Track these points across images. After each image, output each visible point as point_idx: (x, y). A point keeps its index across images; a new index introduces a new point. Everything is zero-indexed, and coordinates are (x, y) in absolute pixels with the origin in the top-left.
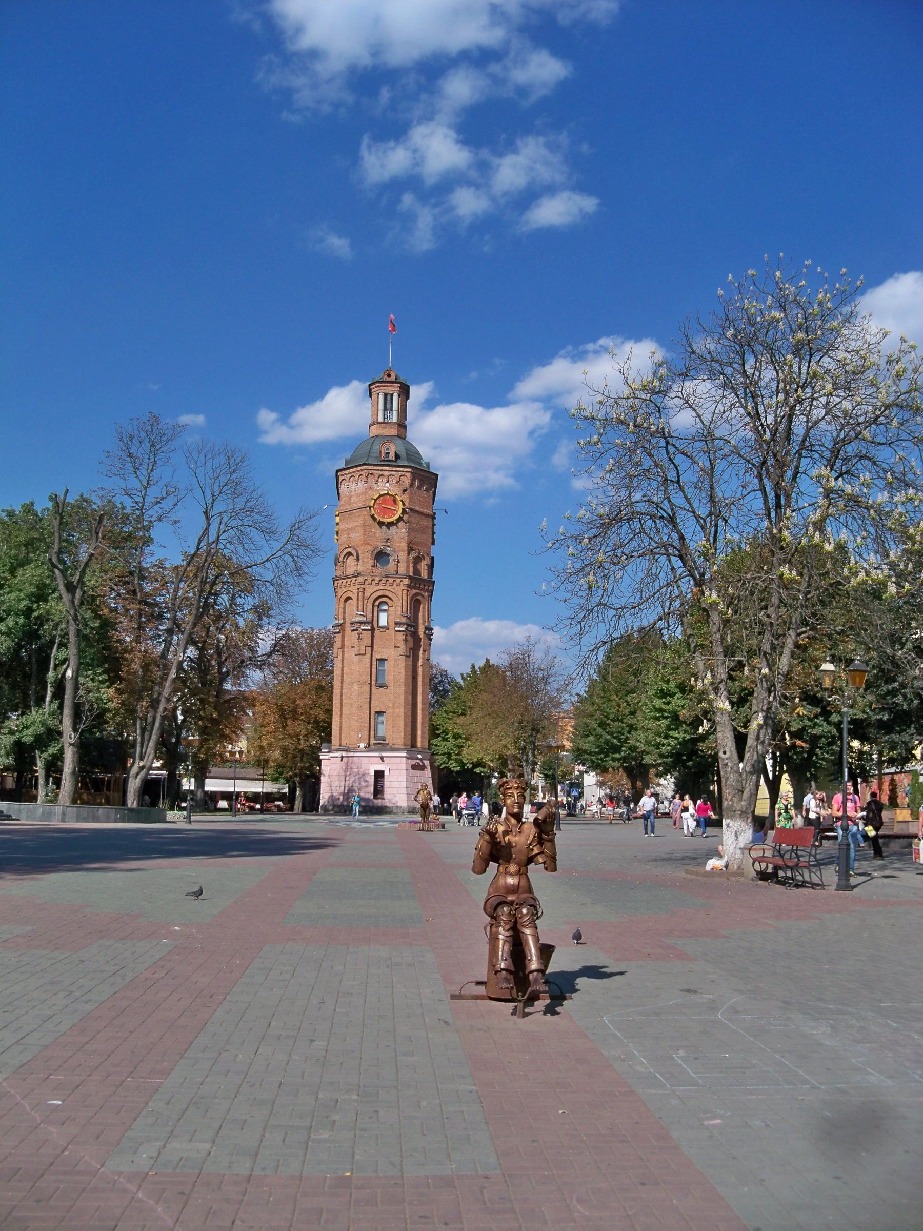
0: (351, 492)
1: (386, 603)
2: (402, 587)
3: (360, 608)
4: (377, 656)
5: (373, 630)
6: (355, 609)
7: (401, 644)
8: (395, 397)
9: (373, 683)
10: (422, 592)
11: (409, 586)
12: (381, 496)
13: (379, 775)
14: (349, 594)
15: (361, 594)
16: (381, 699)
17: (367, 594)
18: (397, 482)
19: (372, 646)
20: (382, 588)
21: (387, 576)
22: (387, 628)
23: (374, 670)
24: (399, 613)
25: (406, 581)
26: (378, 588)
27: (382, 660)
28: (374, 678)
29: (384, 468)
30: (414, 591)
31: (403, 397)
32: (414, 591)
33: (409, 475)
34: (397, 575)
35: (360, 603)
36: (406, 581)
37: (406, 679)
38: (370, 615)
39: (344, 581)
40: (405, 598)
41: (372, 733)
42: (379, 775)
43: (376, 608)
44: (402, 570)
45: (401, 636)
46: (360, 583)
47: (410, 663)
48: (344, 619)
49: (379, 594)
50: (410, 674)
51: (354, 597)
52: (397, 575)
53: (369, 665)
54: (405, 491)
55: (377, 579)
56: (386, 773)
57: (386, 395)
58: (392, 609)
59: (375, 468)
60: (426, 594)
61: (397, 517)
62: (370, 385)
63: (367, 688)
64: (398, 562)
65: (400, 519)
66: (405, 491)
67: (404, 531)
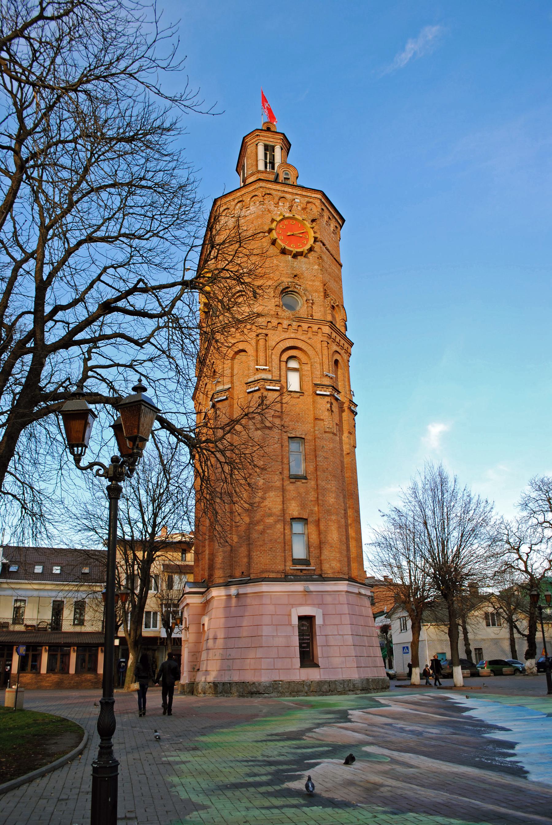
3: (262, 360)
6: (252, 364)
8: (278, 150)
12: (284, 218)
14: (241, 346)
15: (262, 342)
17: (272, 343)
20: (293, 335)
24: (318, 373)
26: (286, 335)
33: (318, 203)
35: (261, 354)
48: (232, 383)
51: (251, 350)
54: (313, 221)
55: (285, 323)
56: (319, 621)
58: (307, 368)
60: (345, 356)
61: (308, 247)
62: (244, 138)
64: (313, 304)
66: (313, 221)
67: (316, 267)
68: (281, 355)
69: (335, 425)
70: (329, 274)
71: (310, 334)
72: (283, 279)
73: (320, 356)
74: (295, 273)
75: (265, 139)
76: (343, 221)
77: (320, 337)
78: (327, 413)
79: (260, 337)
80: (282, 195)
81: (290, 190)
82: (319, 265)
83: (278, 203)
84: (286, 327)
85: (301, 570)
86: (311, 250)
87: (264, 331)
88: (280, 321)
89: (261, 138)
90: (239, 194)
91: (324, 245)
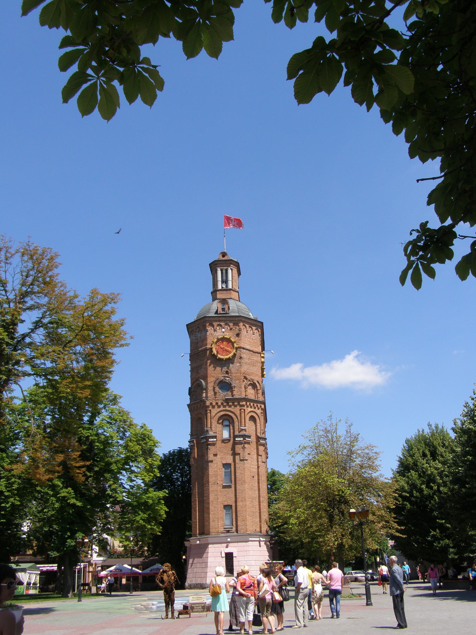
0: (197, 339)
13: (229, 557)
16: (227, 497)
17: (213, 414)
20: (224, 409)
22: (229, 440)
30: (250, 409)
31: (235, 271)
32: (250, 409)
39: (196, 406)
42: (229, 557)
49: (222, 413)
57: (222, 270)
67: (238, 364)
68: (219, 420)
69: (246, 454)
70: (249, 364)
72: (220, 375)
73: (239, 418)
75: (221, 265)
76: (262, 323)
80: (219, 323)
82: (240, 363)
86: (235, 355)
89: (219, 265)
90: (197, 323)
91: (244, 348)
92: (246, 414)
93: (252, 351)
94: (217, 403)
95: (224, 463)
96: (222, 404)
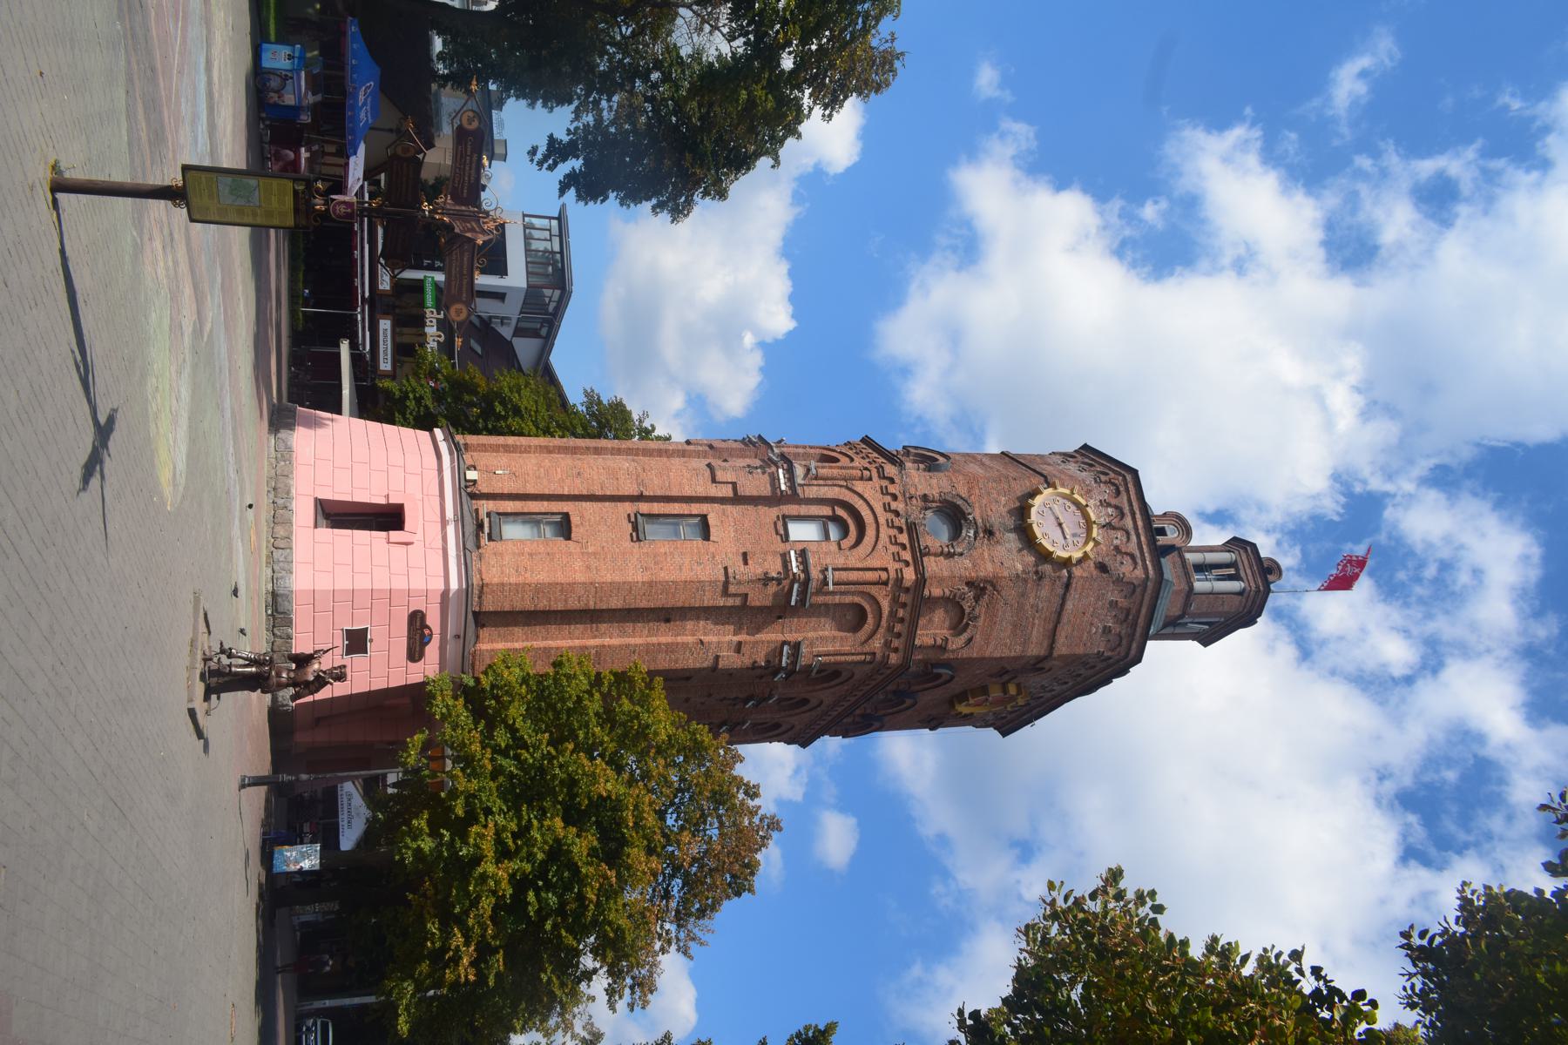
1: (845, 532)
2: (893, 566)
4: (713, 513)
5: (775, 499)
7: (755, 569)
8: (1235, 586)
9: (644, 507)
10: (881, 630)
11: (899, 580)
17: (859, 486)
18: (1117, 548)
19: (737, 499)
20: (882, 520)
21: (912, 529)
23: (676, 508)
25: (909, 575)
27: (705, 530)
28: (657, 508)
29: (1138, 516)
30: (885, 605)
32: (885, 605)
33: (1139, 573)
34: (919, 554)
36: (909, 575)
37: (666, 586)
38: (813, 492)
40: (870, 576)
41: (509, 506)
43: (826, 511)
44: (932, 565)
45: (775, 568)
46: (880, 469)
47: (708, 601)
50: (680, 600)
52: (919, 554)
53: (688, 492)
54: (1102, 567)
55: (899, 506)
56: (395, 535)
58: (834, 547)
59: (1133, 497)
63: (630, 489)
65: (1044, 556)
66: (1102, 567)
67: (1020, 567)
71: (894, 549)
74: (995, 529)
77: (893, 566)
78: (759, 571)
79: (866, 473)
80: (1126, 509)
81: (1140, 523)
83: (1109, 505)
84: (894, 505)
85: (480, 526)
87: (875, 475)
88: (900, 497)
89: (1244, 557)
92: (873, 590)
93: (1058, 622)
94: (895, 497)
95: (711, 521)
96: (897, 514)
